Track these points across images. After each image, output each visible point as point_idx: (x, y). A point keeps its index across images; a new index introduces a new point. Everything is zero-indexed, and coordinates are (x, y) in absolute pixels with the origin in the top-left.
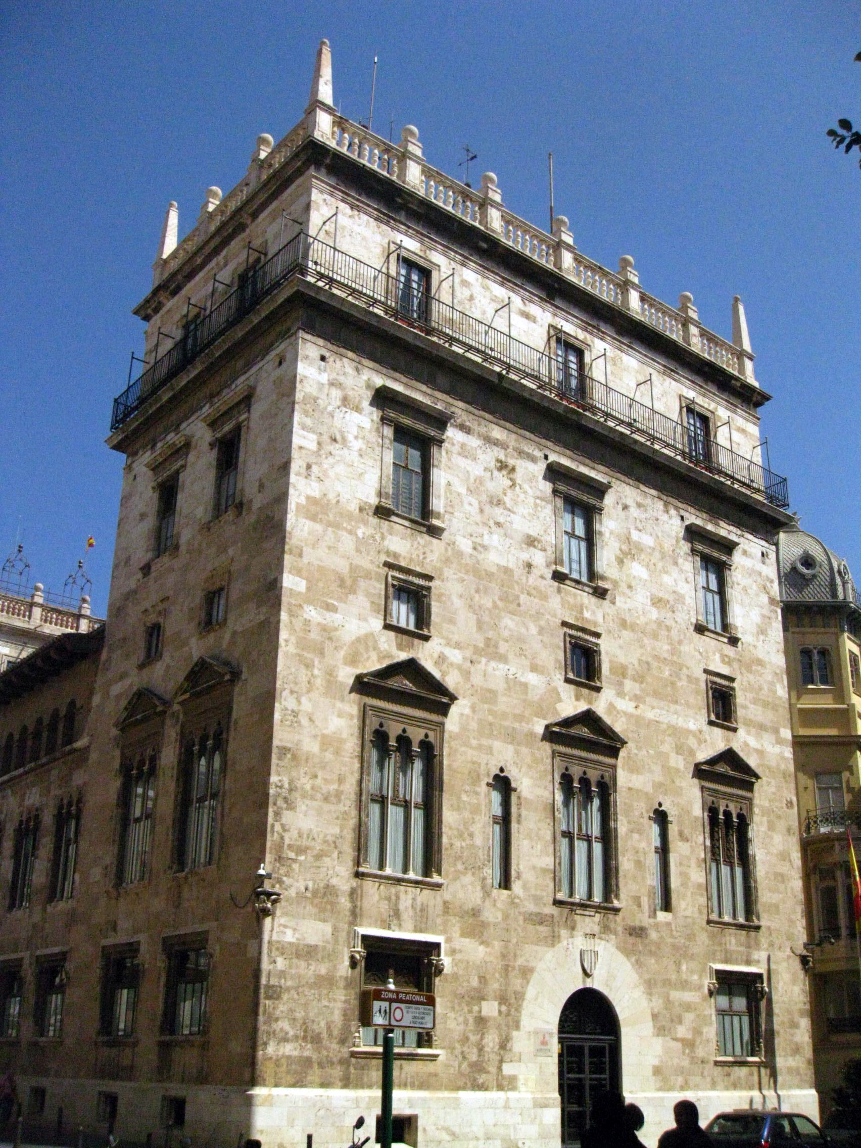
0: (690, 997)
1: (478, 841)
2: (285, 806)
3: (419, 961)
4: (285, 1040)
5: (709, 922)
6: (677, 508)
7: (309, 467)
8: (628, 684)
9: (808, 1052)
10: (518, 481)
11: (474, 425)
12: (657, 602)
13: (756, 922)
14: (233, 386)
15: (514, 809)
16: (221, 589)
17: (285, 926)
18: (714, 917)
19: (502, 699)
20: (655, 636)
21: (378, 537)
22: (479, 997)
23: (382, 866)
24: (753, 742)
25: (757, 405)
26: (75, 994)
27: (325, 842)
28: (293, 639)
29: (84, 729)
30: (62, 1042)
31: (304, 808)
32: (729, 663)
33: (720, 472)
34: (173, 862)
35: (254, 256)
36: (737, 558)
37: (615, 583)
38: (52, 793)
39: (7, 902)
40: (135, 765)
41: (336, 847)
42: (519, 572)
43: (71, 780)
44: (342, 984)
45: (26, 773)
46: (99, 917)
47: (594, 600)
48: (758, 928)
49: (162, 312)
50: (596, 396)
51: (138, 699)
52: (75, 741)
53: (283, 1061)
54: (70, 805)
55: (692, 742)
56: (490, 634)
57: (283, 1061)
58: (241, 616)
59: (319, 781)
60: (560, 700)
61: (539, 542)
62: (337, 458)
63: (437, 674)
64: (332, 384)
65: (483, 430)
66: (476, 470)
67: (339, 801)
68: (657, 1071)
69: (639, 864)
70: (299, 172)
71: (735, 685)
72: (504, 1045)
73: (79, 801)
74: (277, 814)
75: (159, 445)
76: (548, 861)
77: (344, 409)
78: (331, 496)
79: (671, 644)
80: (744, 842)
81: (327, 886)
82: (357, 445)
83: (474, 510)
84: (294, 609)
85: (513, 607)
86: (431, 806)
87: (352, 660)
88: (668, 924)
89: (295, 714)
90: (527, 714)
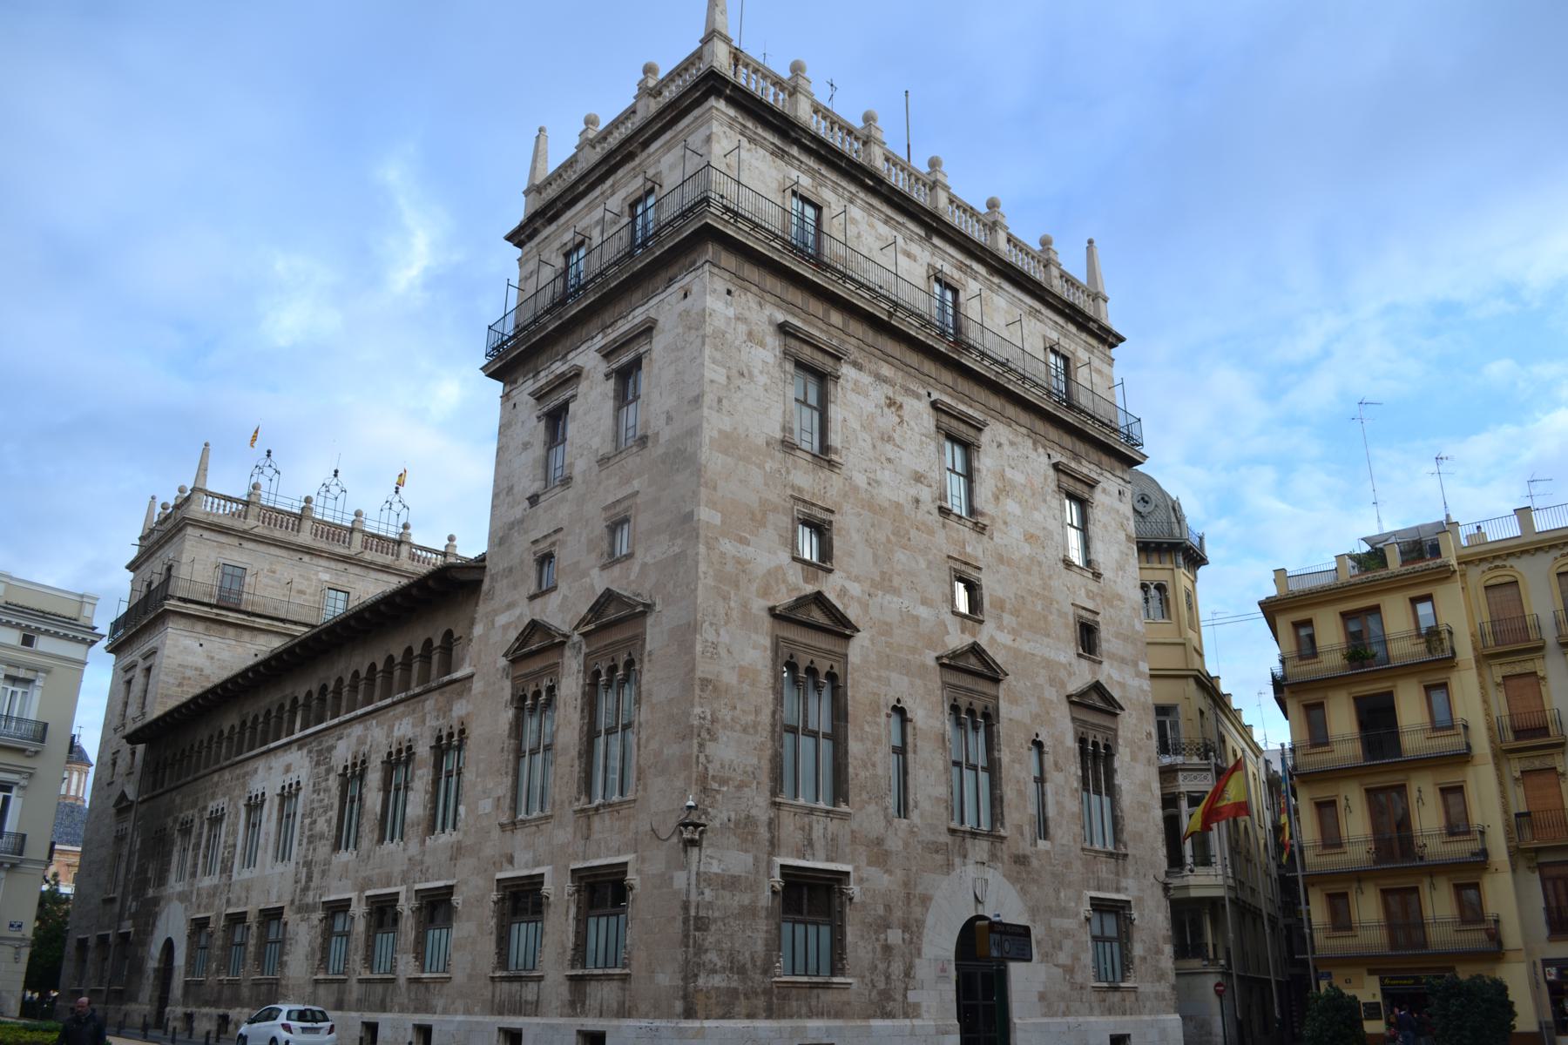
0: (1069, 924)
1: (880, 771)
3: (829, 889)
4: (714, 971)
5: (1083, 849)
6: (1044, 447)
7: (720, 401)
8: (1007, 619)
9: (1172, 978)
12: (1030, 538)
13: (1123, 851)
15: (910, 739)
16: (626, 520)
18: (1087, 845)
20: (1029, 572)
22: (886, 926)
23: (796, 796)
24: (1116, 676)
25: (1112, 346)
26: (462, 929)
28: (711, 572)
29: (463, 659)
32: (1093, 599)
33: (1082, 411)
34: (580, 793)
35: (649, 185)
36: (1098, 497)
37: (993, 519)
39: (376, 837)
40: (529, 695)
42: (908, 507)
44: (763, 914)
45: (394, 704)
46: (489, 851)
47: (974, 535)
48: (1126, 855)
49: (537, 240)
50: (971, 335)
53: (713, 993)
54: (451, 735)
55: (1063, 674)
56: (885, 568)
57: (713, 993)
59: (738, 712)
63: (840, 607)
64: (738, 319)
65: (873, 367)
66: (869, 407)
67: (756, 732)
68: (1042, 997)
69: (1021, 793)
70: (698, 103)
71: (1099, 619)
72: (908, 973)
73: (462, 732)
74: (701, 745)
75: (542, 374)
76: (941, 791)
80: (1110, 773)
81: (748, 817)
82: (763, 379)
83: (867, 446)
85: (904, 541)
86: (838, 739)
87: (765, 592)
88: (1048, 852)
89: (715, 646)
90: (920, 645)
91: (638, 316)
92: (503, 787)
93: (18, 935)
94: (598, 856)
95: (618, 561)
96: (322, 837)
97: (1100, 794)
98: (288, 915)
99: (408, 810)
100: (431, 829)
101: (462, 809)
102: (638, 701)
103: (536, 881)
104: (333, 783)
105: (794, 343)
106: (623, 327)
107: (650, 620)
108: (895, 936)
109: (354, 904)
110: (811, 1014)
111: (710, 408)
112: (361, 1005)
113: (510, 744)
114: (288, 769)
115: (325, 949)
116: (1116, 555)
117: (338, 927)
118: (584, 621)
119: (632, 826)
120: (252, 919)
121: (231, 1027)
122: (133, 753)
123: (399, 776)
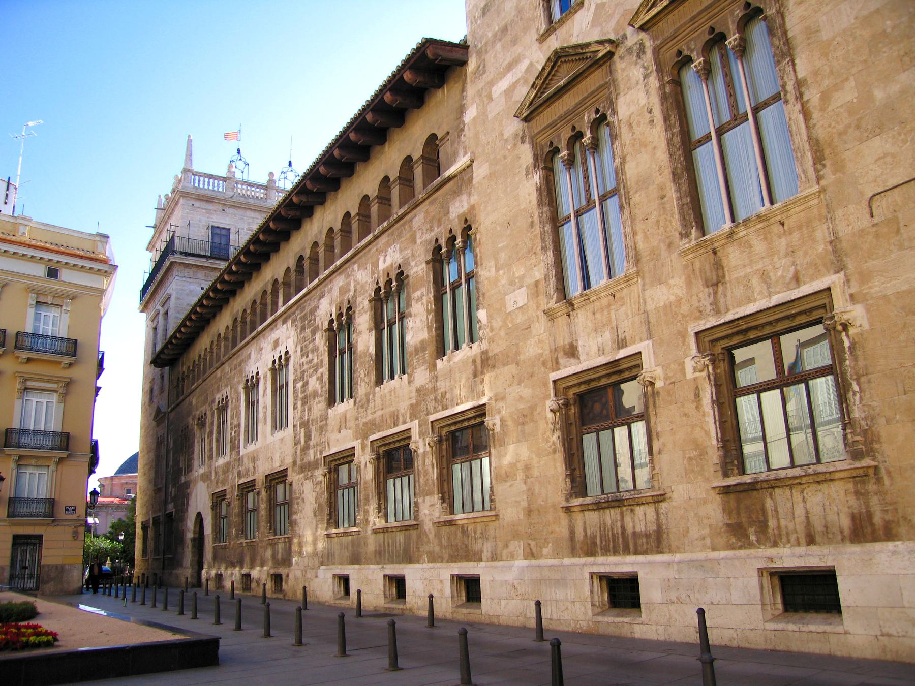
30: (497, 515)
38: (419, 241)
39: (373, 378)
40: (563, 145)
46: (531, 349)
51: (553, 68)
54: (452, 239)
92: (540, 268)
93: (74, 517)
94: (750, 300)
96: (315, 394)
98: (293, 477)
99: (408, 338)
100: (441, 351)
101: (482, 315)
102: (785, 52)
103: (624, 370)
104: (321, 341)
109: (358, 452)
112: (381, 556)
114: (276, 344)
115: (332, 503)
117: (344, 479)
120: (260, 484)
121: (254, 585)
122: (162, 377)
123: (389, 310)
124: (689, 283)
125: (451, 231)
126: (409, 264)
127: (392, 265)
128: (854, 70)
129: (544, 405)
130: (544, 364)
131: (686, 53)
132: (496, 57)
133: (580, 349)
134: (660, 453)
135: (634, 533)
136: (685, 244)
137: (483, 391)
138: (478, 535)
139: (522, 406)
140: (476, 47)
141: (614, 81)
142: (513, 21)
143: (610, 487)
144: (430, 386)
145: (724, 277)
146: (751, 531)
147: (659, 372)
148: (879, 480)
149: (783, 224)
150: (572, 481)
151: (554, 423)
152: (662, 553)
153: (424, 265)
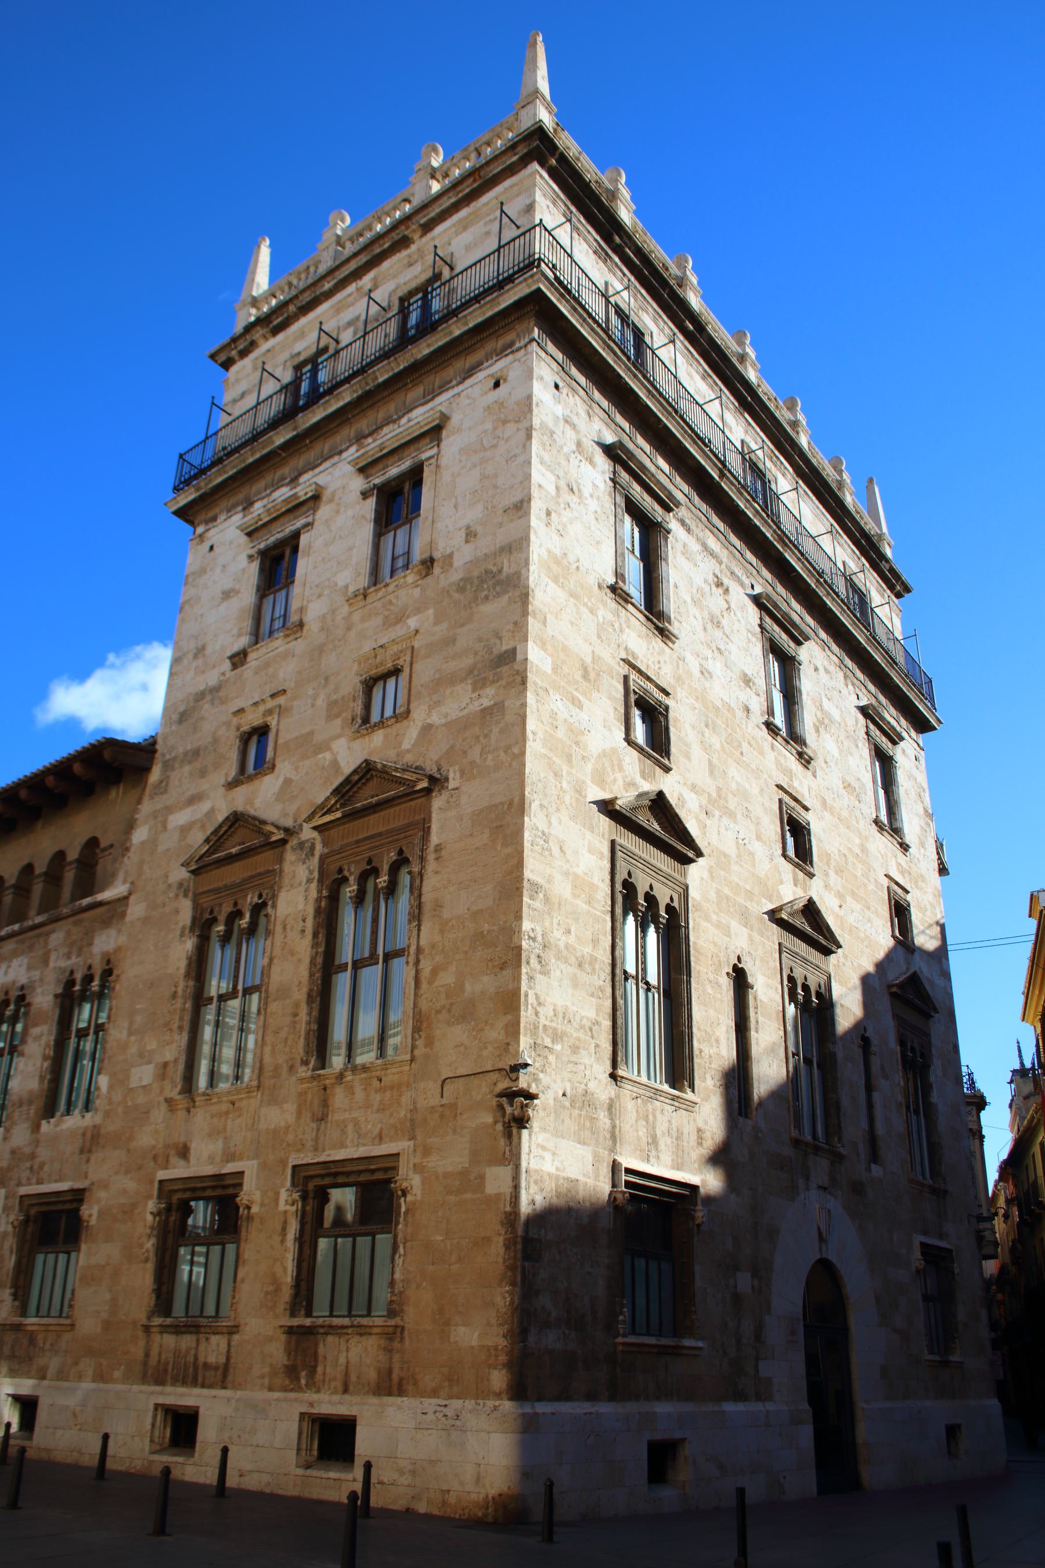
2: (538, 967)
6: (853, 684)
7: (548, 514)
10: (733, 606)
11: (693, 527)
14: (404, 421)
16: (396, 672)
17: (544, 1148)
19: (735, 868)
21: (617, 625)
27: (582, 1027)
28: (540, 735)
29: (114, 875)
31: (558, 973)
32: (902, 872)
38: (52, 964)
40: (222, 918)
41: (592, 1037)
42: (740, 714)
43: (91, 944)
46: (146, 1139)
47: (800, 768)
49: (252, 356)
51: (230, 827)
52: (102, 890)
54: (88, 979)
58: (438, 703)
59: (572, 939)
60: (782, 882)
61: (754, 684)
62: (577, 515)
67: (594, 969)
70: (511, 170)
71: (909, 897)
73: (108, 973)
77: (580, 457)
78: (571, 558)
79: (860, 838)
83: (698, 625)
84: (541, 692)
91: (420, 417)
94: (343, 1145)
95: (382, 724)
97: (917, 1112)
100: (49, 1110)
102: (416, 916)
105: (624, 476)
106: (390, 435)
107: (438, 802)
108: (744, 1281)
110: (662, 1394)
111: (539, 518)
113: (184, 987)
116: (918, 830)
118: (324, 809)
119: (406, 1099)
124: (299, 1113)
125: (90, 967)
126: (34, 989)
127: (14, 983)
128: (457, 957)
129: (146, 1205)
130: (155, 1158)
131: (346, 873)
132: (182, 782)
133: (192, 1151)
134: (243, 1281)
135: (206, 1365)
136: (303, 1072)
137: (87, 1173)
138: (48, 1346)
139: (123, 1201)
140: (164, 755)
141: (281, 871)
142: (206, 747)
143: (194, 1310)
144: (27, 1150)
145: (327, 1116)
146: (303, 1374)
147: (257, 1196)
148: (402, 1339)
149: (381, 1080)
150: (158, 1297)
151: (152, 1228)
152: (225, 1388)
153: (51, 997)
